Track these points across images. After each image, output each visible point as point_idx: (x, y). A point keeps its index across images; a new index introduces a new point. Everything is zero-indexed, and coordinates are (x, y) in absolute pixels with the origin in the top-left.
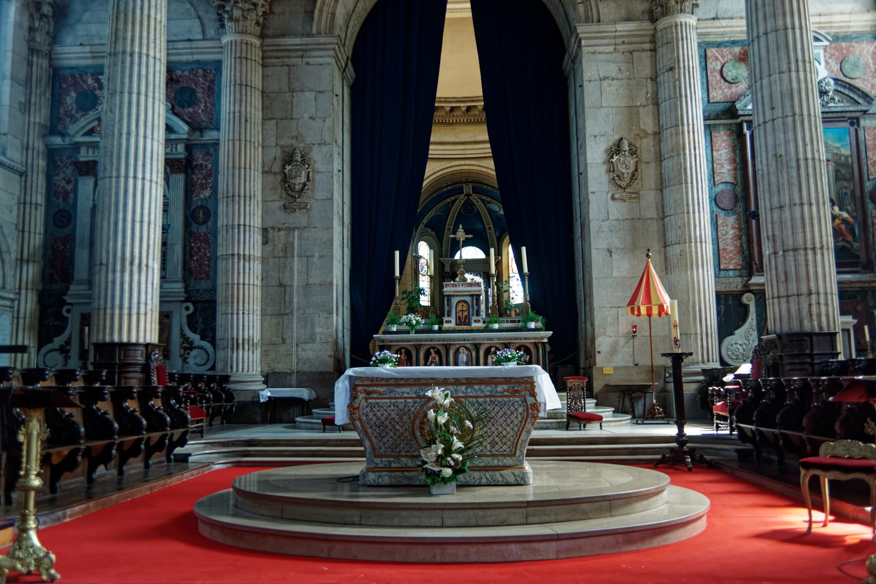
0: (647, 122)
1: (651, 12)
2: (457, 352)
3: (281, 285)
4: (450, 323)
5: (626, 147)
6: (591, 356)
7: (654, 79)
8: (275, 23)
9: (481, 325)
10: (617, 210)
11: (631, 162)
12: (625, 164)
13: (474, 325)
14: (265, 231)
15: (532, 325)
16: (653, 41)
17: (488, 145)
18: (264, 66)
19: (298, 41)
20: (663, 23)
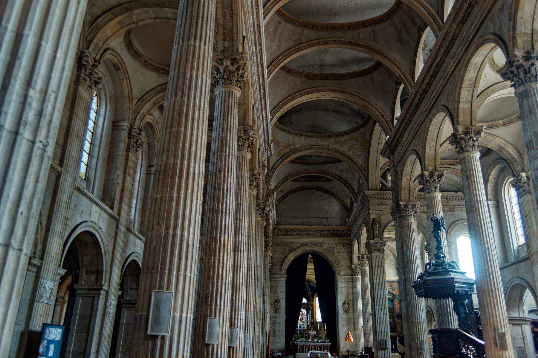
0: (351, 297)
1: (352, 273)
2: (312, 347)
3: (274, 330)
4: (310, 340)
5: (346, 303)
6: (339, 348)
7: (352, 288)
8: (273, 271)
9: (316, 341)
10: (345, 316)
11: (347, 306)
12: (346, 306)
13: (315, 341)
14: (270, 317)
15: (327, 341)
16: (352, 280)
17: (314, 270)
18: (271, 280)
19: (278, 275)
20: (354, 277)
